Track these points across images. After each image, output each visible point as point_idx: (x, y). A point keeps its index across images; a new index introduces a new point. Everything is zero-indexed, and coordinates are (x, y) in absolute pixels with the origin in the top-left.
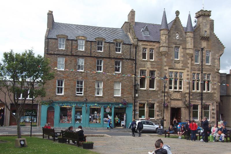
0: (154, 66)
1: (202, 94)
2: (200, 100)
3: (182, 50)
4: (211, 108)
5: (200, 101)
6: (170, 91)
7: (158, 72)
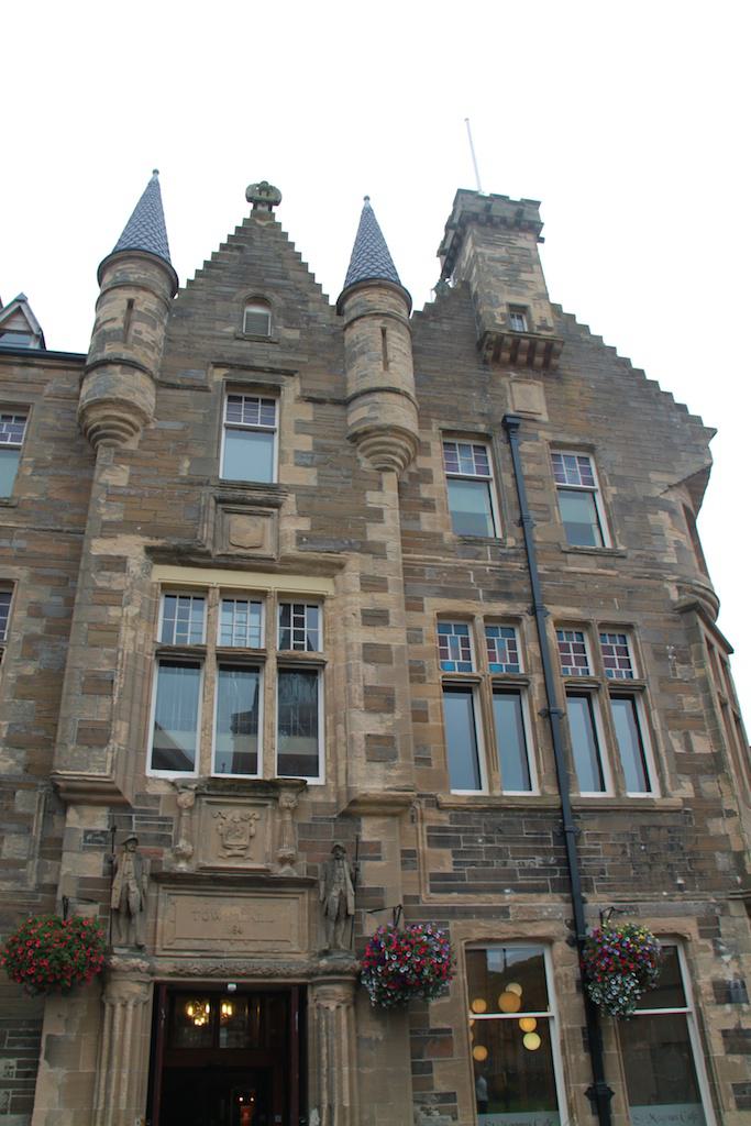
3: (307, 412)
4: (705, 981)
5: (551, 908)
6: (164, 790)
7: (42, 594)
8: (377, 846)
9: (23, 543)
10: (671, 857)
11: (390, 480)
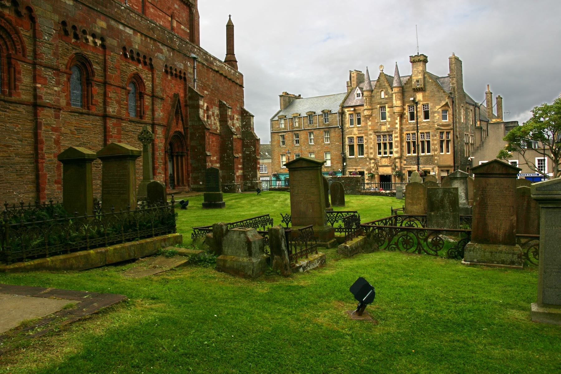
1: (418, 157)
5: (416, 167)
11: (398, 118)
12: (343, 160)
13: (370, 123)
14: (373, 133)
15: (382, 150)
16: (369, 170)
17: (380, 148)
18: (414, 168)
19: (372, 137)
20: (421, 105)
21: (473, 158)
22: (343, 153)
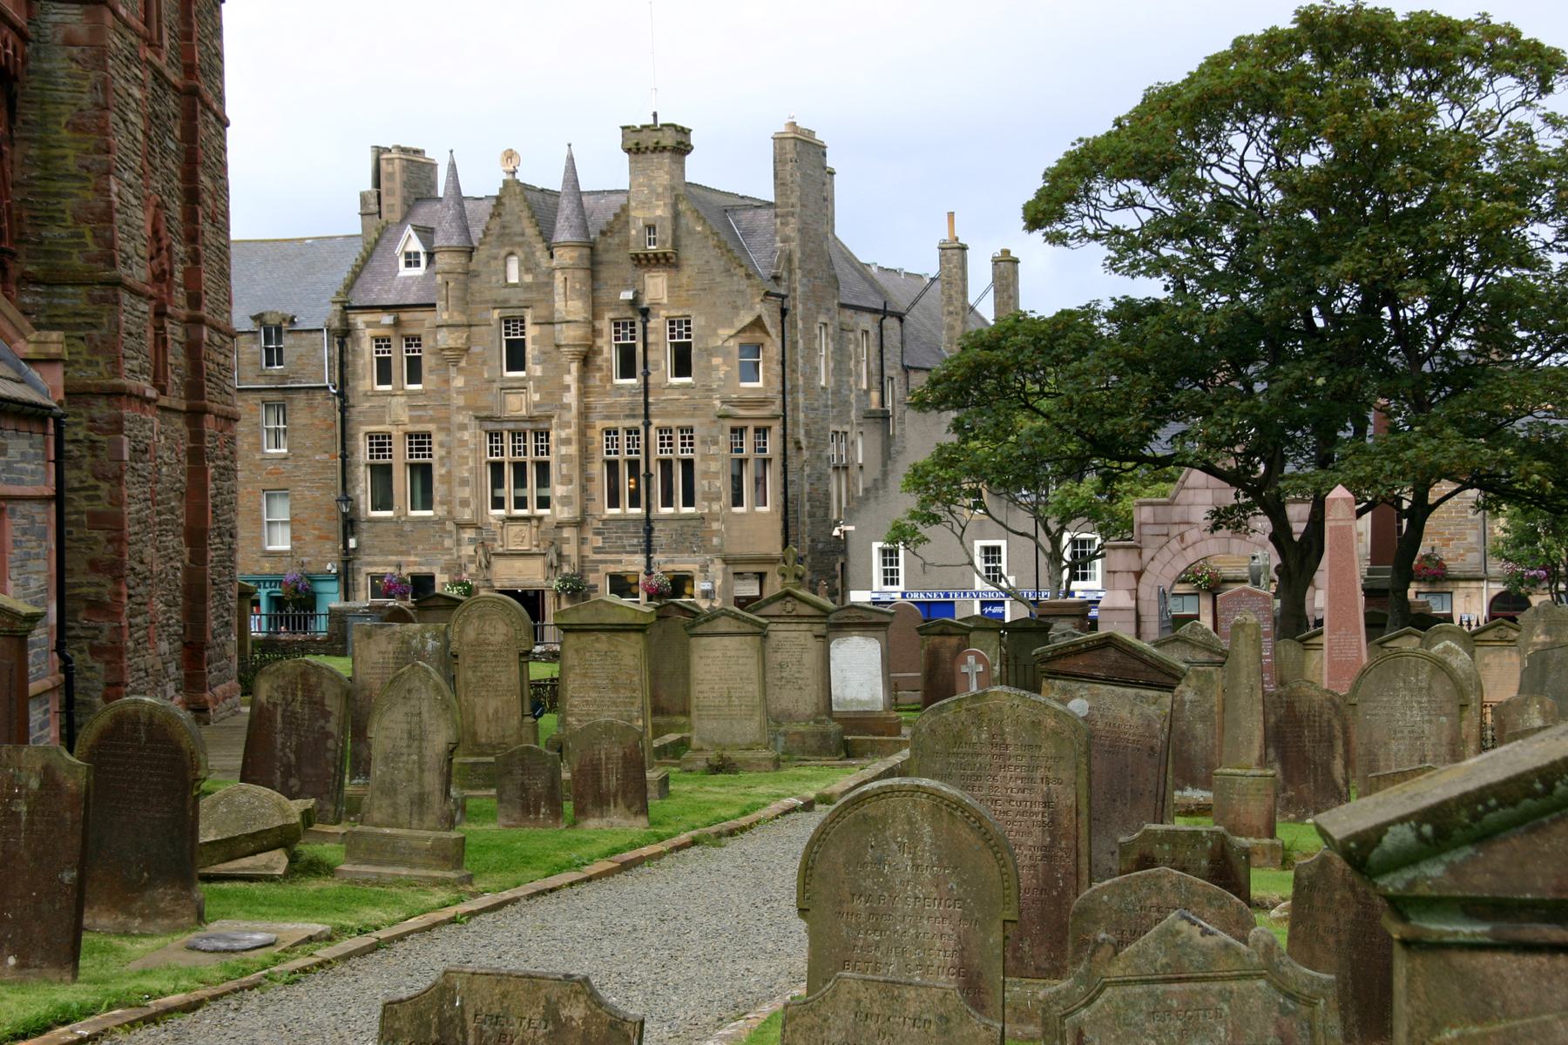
0: (419, 413)
2: (642, 551)
5: (640, 559)
8: (568, 539)
9: (431, 412)
10: (693, 540)
11: (574, 367)
12: (345, 528)
13: (459, 382)
14: (474, 423)
15: (508, 491)
16: (455, 568)
17: (498, 482)
18: (632, 563)
19: (466, 435)
20: (662, 319)
21: (851, 528)
22: (346, 497)
